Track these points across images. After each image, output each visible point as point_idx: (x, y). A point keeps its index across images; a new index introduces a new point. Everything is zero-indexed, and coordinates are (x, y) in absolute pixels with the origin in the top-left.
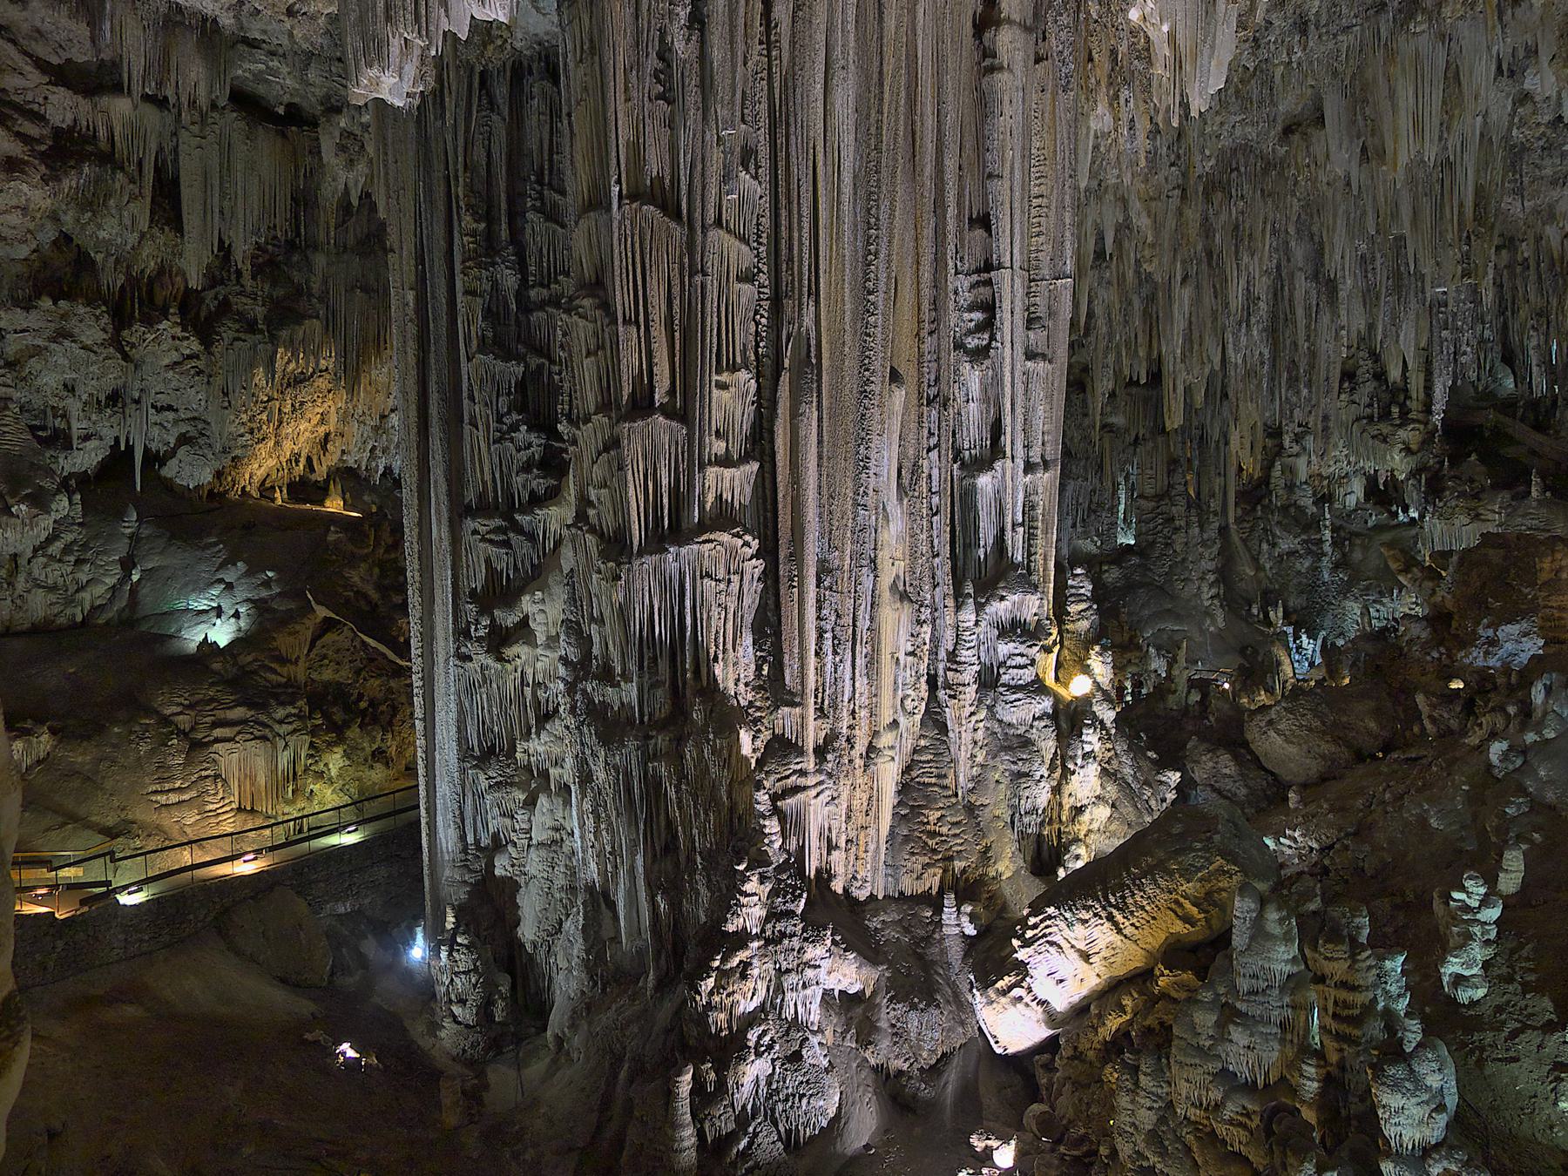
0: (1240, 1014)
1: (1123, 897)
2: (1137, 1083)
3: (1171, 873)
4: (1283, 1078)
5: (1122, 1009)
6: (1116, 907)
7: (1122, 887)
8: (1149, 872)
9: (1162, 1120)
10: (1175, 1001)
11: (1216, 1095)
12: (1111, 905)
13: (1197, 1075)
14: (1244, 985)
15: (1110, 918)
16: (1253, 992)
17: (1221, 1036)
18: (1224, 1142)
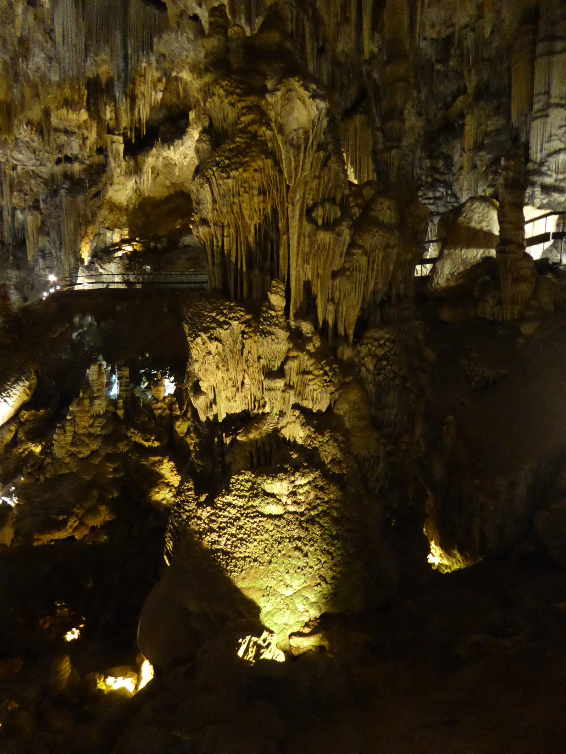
0: (96, 397)
1: (8, 393)
2: (65, 431)
3: (23, 381)
4: (106, 411)
5: (11, 431)
6: (7, 397)
7: (6, 390)
8: (16, 382)
9: (74, 437)
10: (30, 421)
11: (91, 421)
12: (4, 397)
13: (86, 419)
14: (95, 389)
15: (5, 401)
16: (99, 390)
17: (91, 404)
18: (94, 434)
